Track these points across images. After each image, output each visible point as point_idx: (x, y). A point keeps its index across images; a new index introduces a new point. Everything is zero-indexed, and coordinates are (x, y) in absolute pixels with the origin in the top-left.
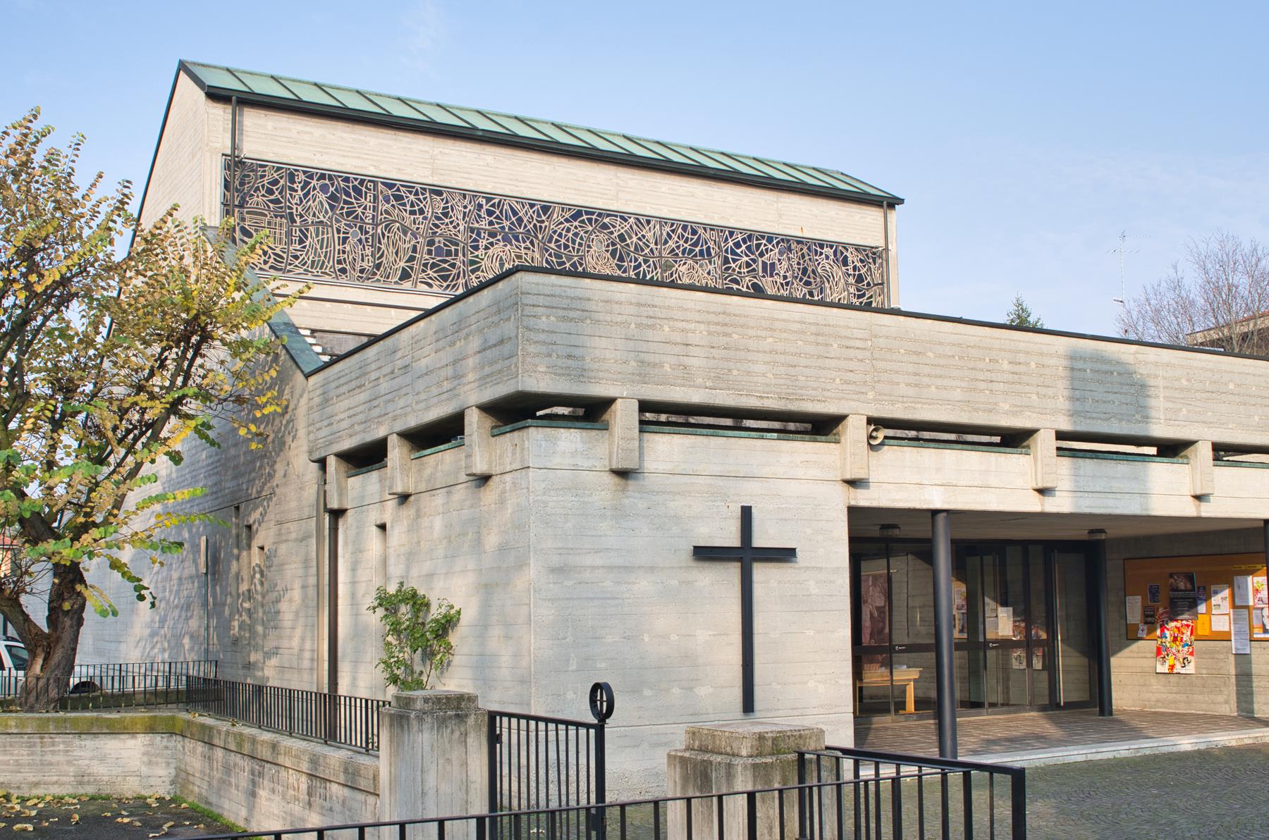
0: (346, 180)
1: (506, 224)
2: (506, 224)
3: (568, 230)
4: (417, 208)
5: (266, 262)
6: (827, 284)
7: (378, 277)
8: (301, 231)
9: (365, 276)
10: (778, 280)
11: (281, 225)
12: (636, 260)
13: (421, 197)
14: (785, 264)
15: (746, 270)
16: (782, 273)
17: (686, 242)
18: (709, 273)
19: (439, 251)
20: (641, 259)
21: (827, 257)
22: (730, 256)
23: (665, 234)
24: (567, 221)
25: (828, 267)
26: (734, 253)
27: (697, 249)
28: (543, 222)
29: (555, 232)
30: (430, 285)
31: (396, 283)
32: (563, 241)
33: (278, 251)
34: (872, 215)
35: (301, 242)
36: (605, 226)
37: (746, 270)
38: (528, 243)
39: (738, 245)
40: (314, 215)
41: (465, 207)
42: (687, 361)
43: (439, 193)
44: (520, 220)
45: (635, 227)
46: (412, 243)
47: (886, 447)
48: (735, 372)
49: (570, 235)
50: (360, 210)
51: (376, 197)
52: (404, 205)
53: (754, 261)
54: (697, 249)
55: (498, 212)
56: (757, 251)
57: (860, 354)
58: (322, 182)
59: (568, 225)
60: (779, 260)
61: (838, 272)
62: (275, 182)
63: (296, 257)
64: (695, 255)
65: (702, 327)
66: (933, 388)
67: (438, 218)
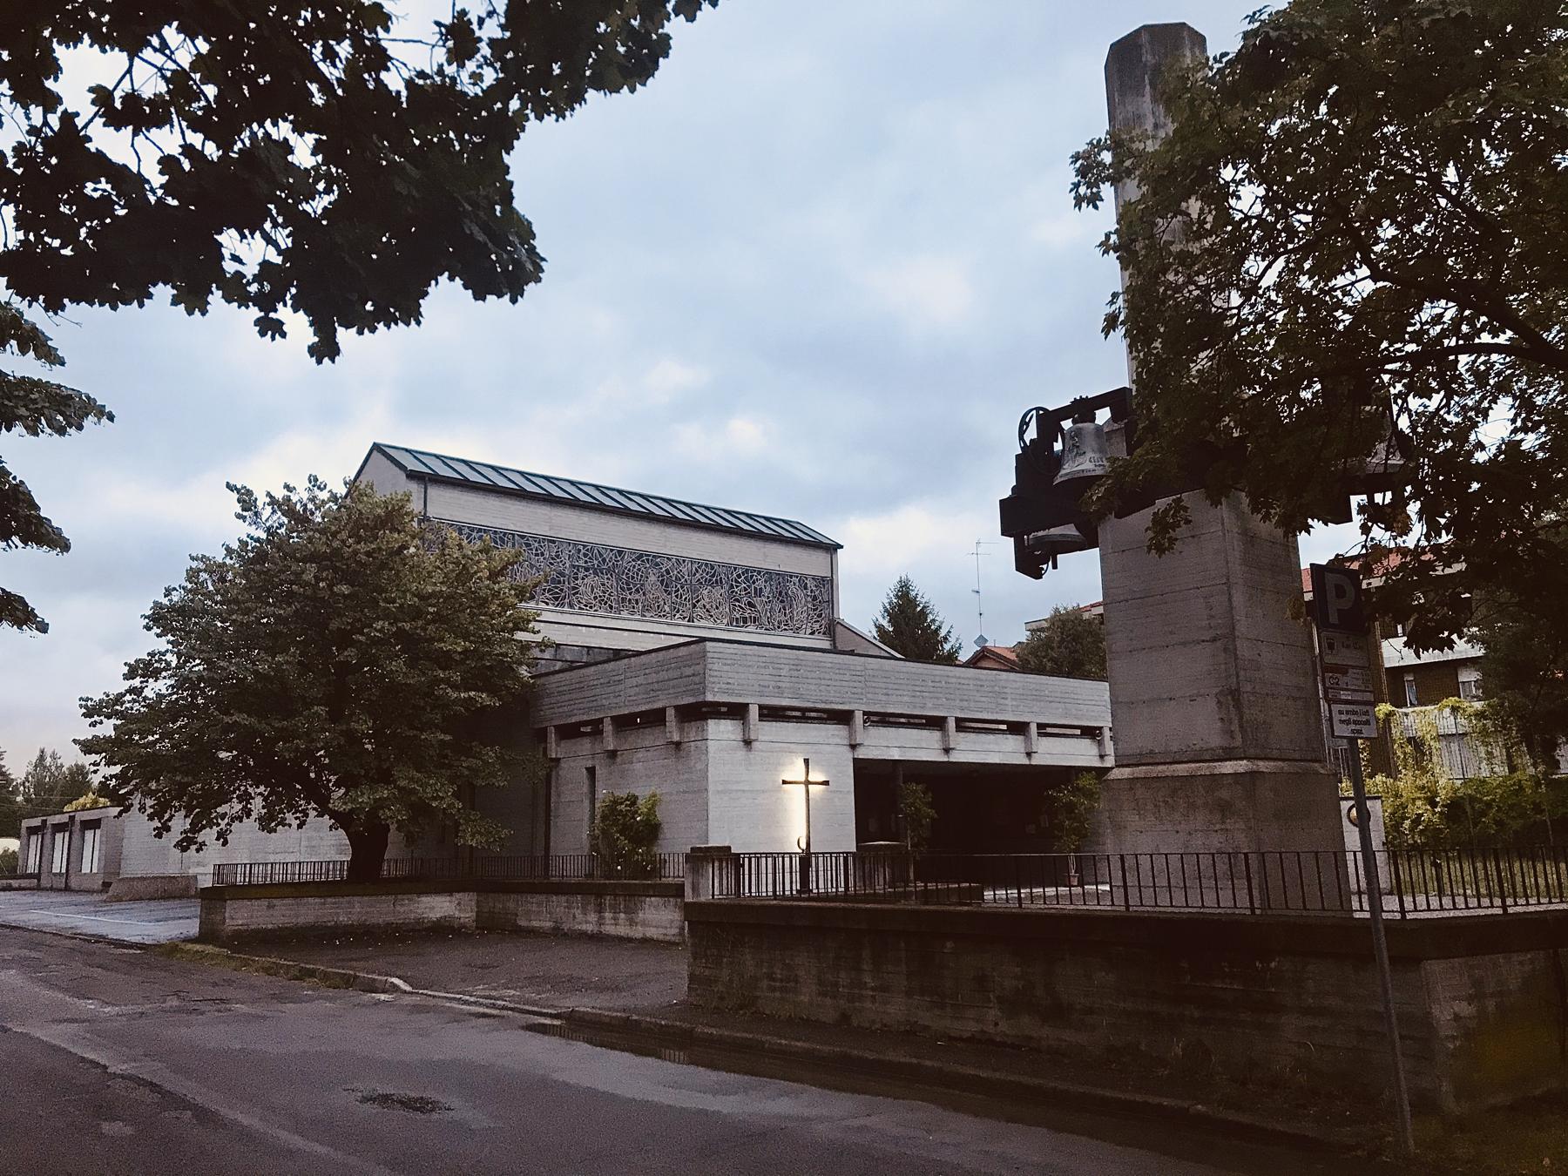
14: (768, 589)
19: (553, 580)
21: (795, 584)
30: (547, 604)
36: (657, 564)
39: (739, 576)
43: (554, 542)
44: (604, 560)
61: (801, 594)
67: (553, 559)
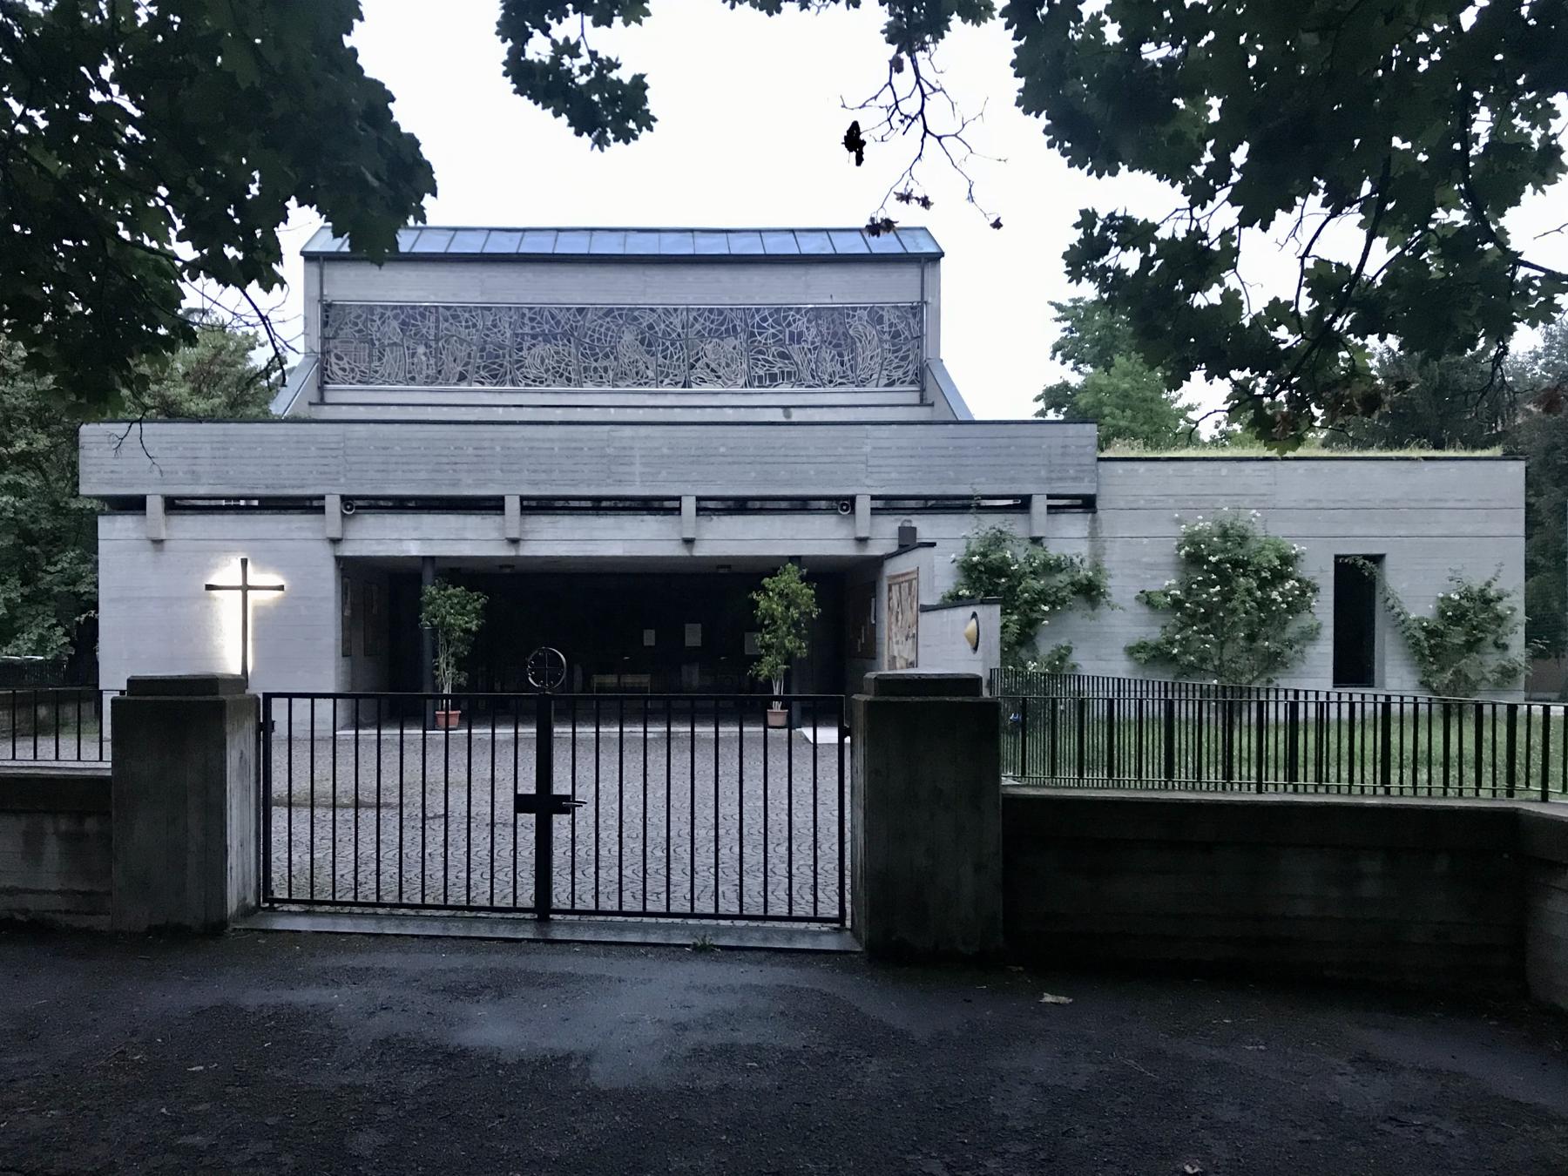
0: (413, 308)
1: (546, 327)
2: (546, 327)
3: (601, 326)
4: (470, 323)
5: (353, 378)
6: (858, 344)
7: (440, 381)
8: (380, 352)
9: (430, 380)
10: (806, 347)
11: (364, 348)
12: (664, 344)
13: (474, 314)
14: (813, 331)
15: (772, 341)
16: (810, 339)
17: (712, 322)
18: (734, 348)
19: (489, 355)
20: (668, 343)
21: (860, 319)
22: (756, 330)
23: (691, 318)
24: (600, 318)
25: (860, 328)
26: (760, 327)
27: (723, 328)
28: (578, 321)
29: (589, 329)
30: (483, 383)
31: (455, 384)
32: (596, 335)
33: (362, 369)
34: (910, 274)
35: (380, 359)
36: (635, 319)
37: (772, 341)
38: (565, 341)
39: (764, 319)
40: (389, 338)
41: (511, 318)
42: (194, 468)
43: (489, 309)
44: (558, 323)
45: (663, 316)
46: (468, 351)
47: (358, 516)
48: (232, 473)
49: (603, 330)
50: (424, 331)
51: (437, 320)
52: (460, 322)
53: (780, 332)
54: (723, 328)
55: (539, 318)
56: (784, 321)
57: (334, 453)
58: (395, 311)
59: (600, 321)
60: (807, 328)
61: (872, 332)
62: (359, 317)
63: (376, 372)
64: (721, 333)
65: (207, 445)
66: (400, 473)
67: (488, 329)
